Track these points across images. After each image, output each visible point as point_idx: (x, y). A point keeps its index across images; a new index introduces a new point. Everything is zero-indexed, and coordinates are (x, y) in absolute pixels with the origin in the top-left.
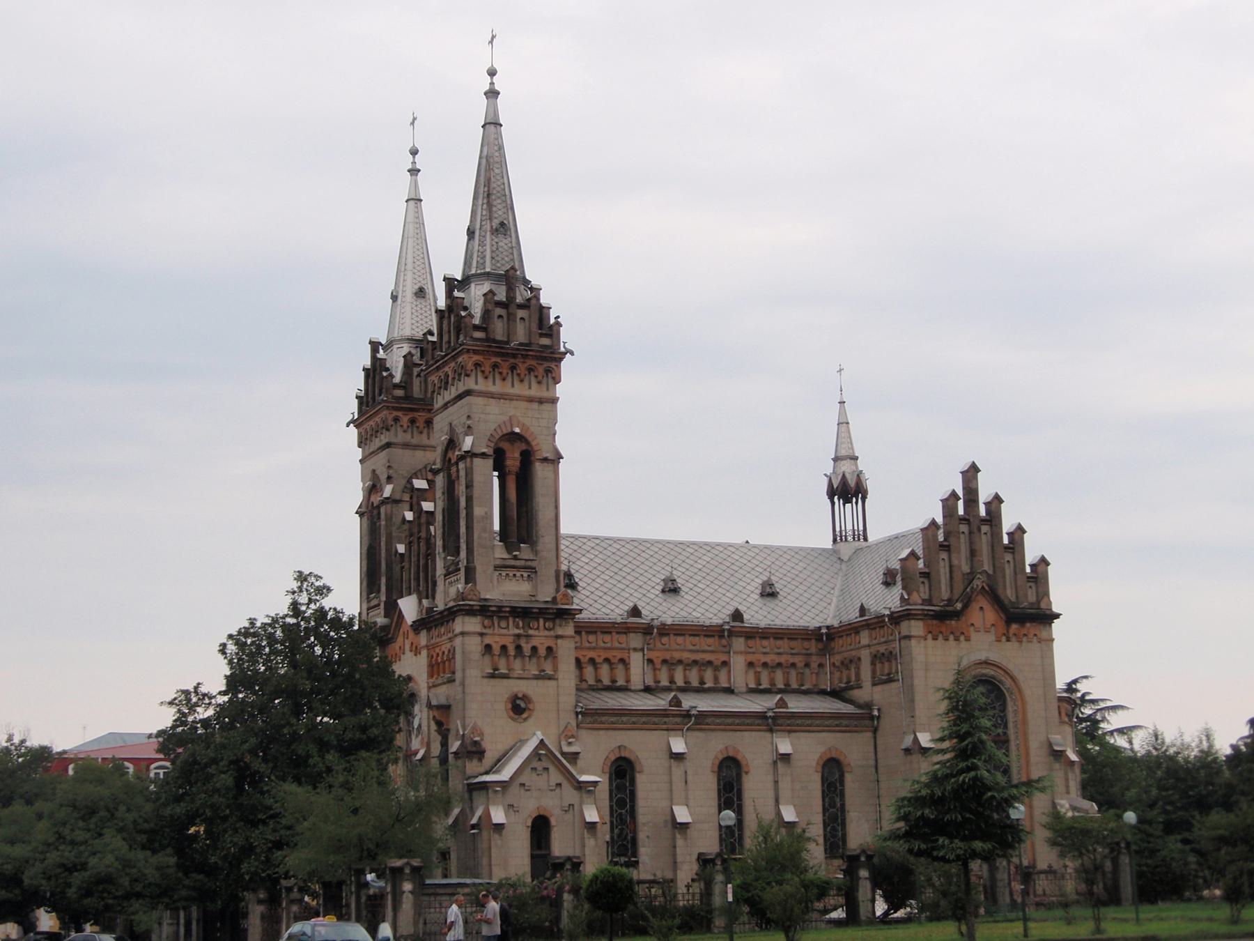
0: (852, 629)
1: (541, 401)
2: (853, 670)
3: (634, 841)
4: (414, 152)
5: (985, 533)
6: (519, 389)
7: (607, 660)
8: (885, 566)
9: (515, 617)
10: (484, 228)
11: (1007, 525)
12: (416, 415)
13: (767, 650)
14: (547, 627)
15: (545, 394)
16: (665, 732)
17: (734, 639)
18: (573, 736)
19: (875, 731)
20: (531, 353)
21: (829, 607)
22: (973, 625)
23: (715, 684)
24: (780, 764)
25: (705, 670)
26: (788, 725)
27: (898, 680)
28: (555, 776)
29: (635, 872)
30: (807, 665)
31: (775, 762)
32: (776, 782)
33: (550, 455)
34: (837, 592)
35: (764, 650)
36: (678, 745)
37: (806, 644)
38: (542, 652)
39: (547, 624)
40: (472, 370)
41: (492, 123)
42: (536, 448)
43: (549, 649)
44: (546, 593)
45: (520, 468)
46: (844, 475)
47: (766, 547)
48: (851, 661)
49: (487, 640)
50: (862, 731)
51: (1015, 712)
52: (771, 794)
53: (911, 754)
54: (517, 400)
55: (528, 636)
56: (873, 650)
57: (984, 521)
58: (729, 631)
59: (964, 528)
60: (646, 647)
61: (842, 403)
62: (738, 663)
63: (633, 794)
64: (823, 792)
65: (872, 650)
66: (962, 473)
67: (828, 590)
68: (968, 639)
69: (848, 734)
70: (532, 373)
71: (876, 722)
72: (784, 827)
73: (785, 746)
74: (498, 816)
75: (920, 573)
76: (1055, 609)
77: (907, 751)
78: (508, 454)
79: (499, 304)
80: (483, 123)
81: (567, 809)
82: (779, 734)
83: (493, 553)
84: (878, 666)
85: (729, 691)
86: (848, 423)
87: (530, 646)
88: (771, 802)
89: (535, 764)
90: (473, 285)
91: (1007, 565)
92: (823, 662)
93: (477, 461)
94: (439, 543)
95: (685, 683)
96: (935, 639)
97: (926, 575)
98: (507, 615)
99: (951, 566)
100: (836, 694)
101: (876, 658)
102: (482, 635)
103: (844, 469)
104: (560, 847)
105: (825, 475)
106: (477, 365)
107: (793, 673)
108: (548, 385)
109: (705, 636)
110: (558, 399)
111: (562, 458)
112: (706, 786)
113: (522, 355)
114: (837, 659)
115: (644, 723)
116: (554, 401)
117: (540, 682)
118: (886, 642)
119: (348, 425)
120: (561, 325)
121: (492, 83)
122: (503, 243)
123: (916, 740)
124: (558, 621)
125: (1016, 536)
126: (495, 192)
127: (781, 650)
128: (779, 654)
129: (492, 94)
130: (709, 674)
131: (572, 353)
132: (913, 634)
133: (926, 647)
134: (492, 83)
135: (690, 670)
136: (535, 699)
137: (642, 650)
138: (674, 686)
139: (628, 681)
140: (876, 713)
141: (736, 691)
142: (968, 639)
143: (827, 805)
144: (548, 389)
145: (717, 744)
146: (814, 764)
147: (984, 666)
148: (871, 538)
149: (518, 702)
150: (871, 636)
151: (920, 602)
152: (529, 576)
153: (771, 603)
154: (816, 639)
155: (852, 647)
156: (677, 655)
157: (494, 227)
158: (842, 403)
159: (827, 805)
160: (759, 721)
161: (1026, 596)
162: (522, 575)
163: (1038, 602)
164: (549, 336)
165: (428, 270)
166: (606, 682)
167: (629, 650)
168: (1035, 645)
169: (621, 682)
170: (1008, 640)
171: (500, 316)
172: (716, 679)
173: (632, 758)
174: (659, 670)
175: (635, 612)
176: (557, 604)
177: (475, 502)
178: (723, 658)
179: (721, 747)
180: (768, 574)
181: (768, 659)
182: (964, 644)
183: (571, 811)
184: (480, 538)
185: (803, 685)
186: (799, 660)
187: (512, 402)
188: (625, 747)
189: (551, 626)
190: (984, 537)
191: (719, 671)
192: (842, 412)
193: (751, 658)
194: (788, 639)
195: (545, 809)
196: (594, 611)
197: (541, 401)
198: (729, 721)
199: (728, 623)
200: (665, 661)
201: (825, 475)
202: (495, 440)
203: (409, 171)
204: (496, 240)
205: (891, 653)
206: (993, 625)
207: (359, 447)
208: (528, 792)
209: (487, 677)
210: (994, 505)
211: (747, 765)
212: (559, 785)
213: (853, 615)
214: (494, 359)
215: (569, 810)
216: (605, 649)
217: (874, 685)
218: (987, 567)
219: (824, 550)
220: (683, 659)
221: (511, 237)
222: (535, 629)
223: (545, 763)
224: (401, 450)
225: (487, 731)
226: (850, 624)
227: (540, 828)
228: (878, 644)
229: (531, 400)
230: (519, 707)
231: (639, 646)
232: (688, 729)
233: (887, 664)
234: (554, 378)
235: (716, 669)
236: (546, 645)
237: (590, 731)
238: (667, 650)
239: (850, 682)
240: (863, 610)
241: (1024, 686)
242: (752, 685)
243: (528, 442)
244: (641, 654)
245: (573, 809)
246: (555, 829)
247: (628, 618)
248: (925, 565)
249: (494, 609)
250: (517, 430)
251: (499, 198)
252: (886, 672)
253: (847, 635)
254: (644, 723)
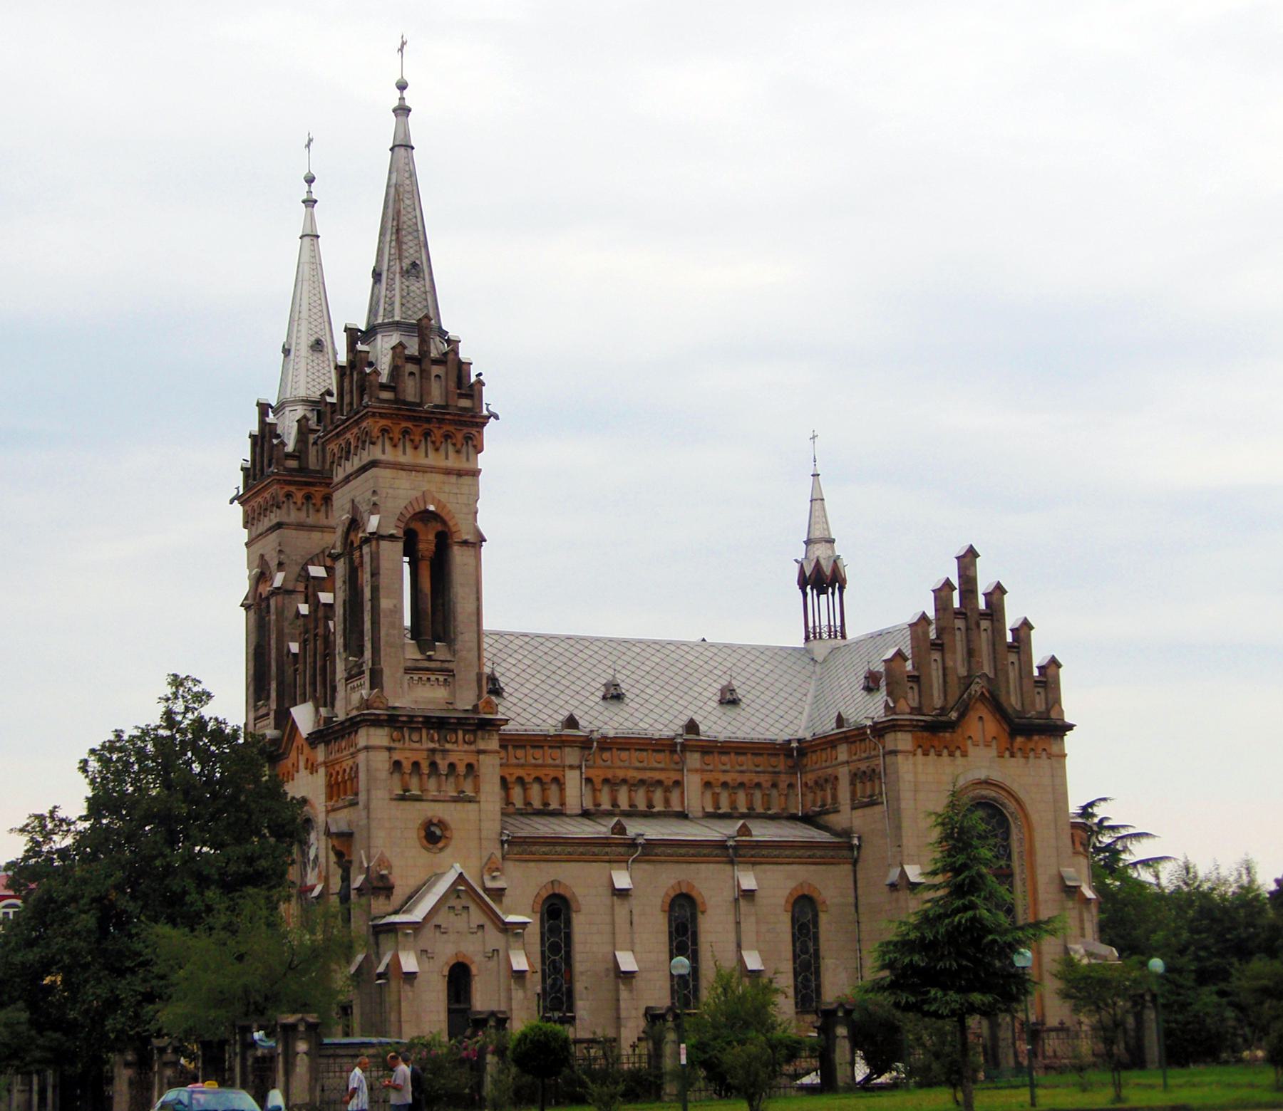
0: (826, 743)
1: (460, 474)
2: (829, 791)
3: (570, 994)
4: (310, 180)
5: (985, 630)
6: (433, 459)
7: (538, 780)
8: (866, 668)
9: (428, 729)
10: (392, 269)
11: (1011, 619)
12: (313, 489)
13: (728, 767)
14: (467, 739)
15: (464, 465)
16: (607, 864)
17: (688, 754)
18: (497, 869)
19: (855, 863)
20: (448, 417)
21: (800, 717)
22: (970, 737)
23: (666, 808)
24: (742, 902)
25: (653, 791)
26: (752, 856)
27: (882, 803)
28: (476, 916)
29: (571, 1029)
30: (774, 785)
31: (736, 900)
32: (738, 923)
33: (470, 538)
34: (809, 699)
35: (724, 768)
36: (622, 880)
37: (773, 760)
38: (461, 769)
39: (467, 736)
40: (378, 437)
41: (402, 146)
42: (454, 529)
43: (470, 767)
44: (466, 700)
45: (435, 553)
46: (818, 563)
47: (726, 646)
48: (826, 781)
49: (396, 756)
50: (839, 864)
51: (1021, 841)
52: (732, 937)
53: (897, 890)
54: (431, 472)
55: (445, 751)
56: (853, 767)
57: (983, 615)
58: (682, 744)
59: (960, 623)
60: (584, 764)
61: (815, 475)
62: (693, 783)
63: (568, 937)
64: (793, 935)
65: (851, 768)
66: (958, 558)
67: (799, 696)
68: (964, 755)
69: (823, 867)
70: (449, 441)
71: (855, 853)
72: (747, 976)
73: (748, 881)
74: (409, 963)
75: (908, 677)
76: (1068, 719)
77: (893, 886)
78: (421, 537)
79: (410, 359)
80: (391, 145)
81: (490, 955)
82: (741, 866)
83: (404, 653)
84: (859, 786)
85: (683, 816)
86: (823, 500)
87: (447, 762)
88: (733, 946)
89: (453, 902)
90: (379, 337)
91: (1010, 668)
92: (793, 781)
93: (384, 545)
94: (339, 641)
95: (631, 806)
96: (926, 754)
97: (915, 679)
98: (420, 726)
99: (944, 669)
100: (808, 819)
101: (854, 777)
102: (389, 749)
103: (818, 553)
104: (483, 999)
105: (796, 561)
106: (384, 431)
107: (758, 795)
108: (468, 454)
109: (654, 751)
110: (479, 471)
111: (485, 541)
112: (655, 929)
113: (437, 419)
114: (810, 778)
115: (582, 854)
116: (475, 473)
117: (459, 805)
118: (867, 758)
119: (231, 502)
120: (483, 384)
121: (402, 99)
122: (415, 287)
123: (903, 874)
124: (479, 733)
125: (1022, 633)
126: (405, 227)
127: (744, 768)
128: (742, 772)
129: (402, 111)
130: (658, 796)
131: (497, 417)
132: (900, 748)
133: (915, 764)
134: (402, 99)
135: (636, 791)
136: (453, 825)
137: (580, 767)
138: (617, 810)
139: (563, 804)
140: (856, 842)
141: (690, 815)
142: (964, 755)
143: (798, 949)
144: (468, 459)
145: (668, 878)
146: (783, 901)
147: (984, 786)
148: (850, 635)
149: (433, 829)
151: (908, 710)
152: (445, 679)
153: (731, 712)
154: (785, 755)
155: (828, 764)
156: (621, 774)
157: (404, 268)
158: (815, 475)
159: (798, 949)
160: (717, 852)
161: (1033, 704)
162: (437, 679)
163: (1048, 711)
164: (469, 396)
165: (326, 319)
166: (537, 804)
167: (564, 768)
168: (1044, 762)
169: (554, 805)
170: (1012, 755)
171: (412, 374)
172: (667, 802)
173: (568, 895)
174: (600, 790)
175: (571, 722)
176: (479, 713)
177: (382, 592)
178: (675, 776)
179: (673, 882)
180: (728, 678)
181: (727, 778)
182: (960, 760)
183: (495, 958)
184: (388, 635)
185: (769, 809)
186: (764, 779)
187: (426, 474)
188: (559, 882)
189: (472, 739)
190: (984, 635)
191: (671, 792)
192: (816, 487)
193: (708, 777)
194: (753, 754)
195: (464, 955)
196: (523, 721)
197: (460, 474)
198: (683, 851)
199: (681, 735)
200: (606, 781)
201: (796, 561)
202: (405, 520)
203: (304, 202)
204: (407, 283)
205: (874, 770)
206: (994, 738)
207: (245, 527)
208: (445, 936)
209: (395, 799)
210: (995, 597)
211: (703, 903)
212: (481, 927)
213: (827, 726)
214: (404, 424)
215: (493, 956)
216: (536, 766)
217: (853, 808)
218: (987, 669)
219: (794, 649)
220: (628, 778)
221: (424, 280)
222: (454, 743)
223: (465, 901)
224: (294, 532)
225: (396, 862)
226: (824, 737)
227: (459, 977)
228: (859, 760)
229: (448, 472)
230: (434, 835)
231: (576, 763)
232: (633, 861)
233: (868, 784)
234: (475, 447)
235: (667, 790)
236: (465, 762)
237: (517, 863)
238: (609, 767)
239: (825, 805)
240: (840, 720)
241: (1030, 808)
242: (710, 809)
243: (444, 522)
244: (577, 773)
245: (498, 955)
246: (476, 978)
247: (562, 730)
248: (914, 667)
249: (404, 719)
250: (432, 508)
251: (410, 233)
252: (868, 792)
253: (822, 750)
254: (582, 854)
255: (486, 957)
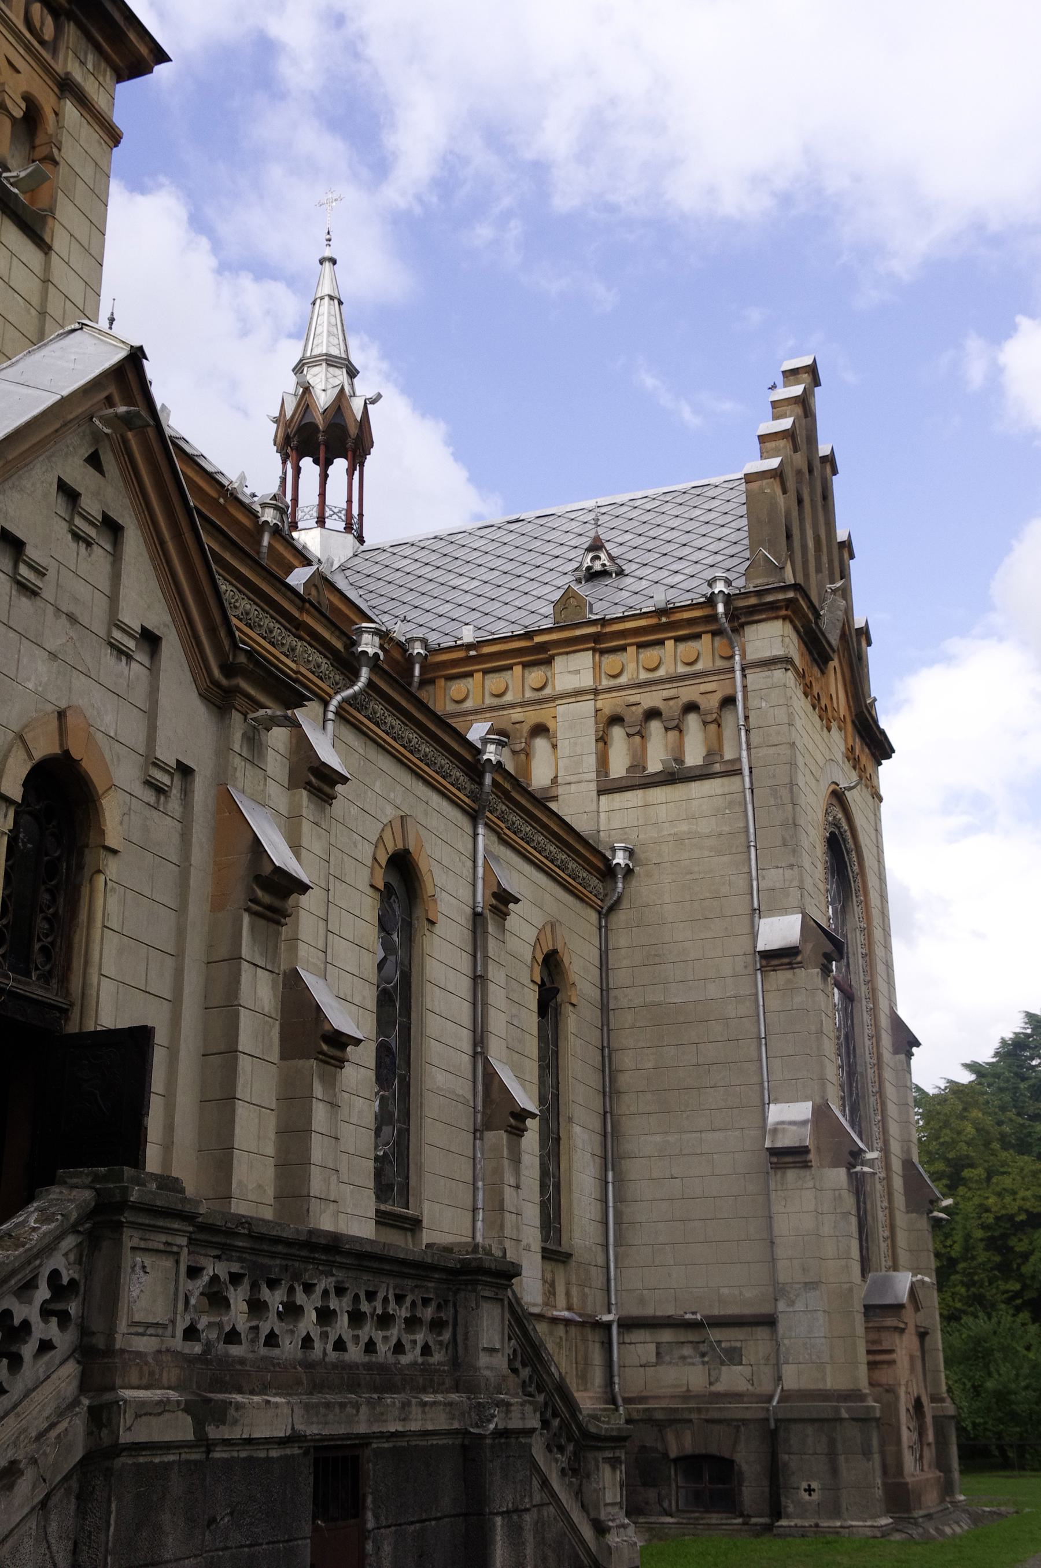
8: (592, 534)
65: (599, 704)
150: (597, 668)
183: (174, 805)
208: (25, 603)
212: (150, 640)
245: (186, 793)
246: (112, 867)
255: (149, 783)
